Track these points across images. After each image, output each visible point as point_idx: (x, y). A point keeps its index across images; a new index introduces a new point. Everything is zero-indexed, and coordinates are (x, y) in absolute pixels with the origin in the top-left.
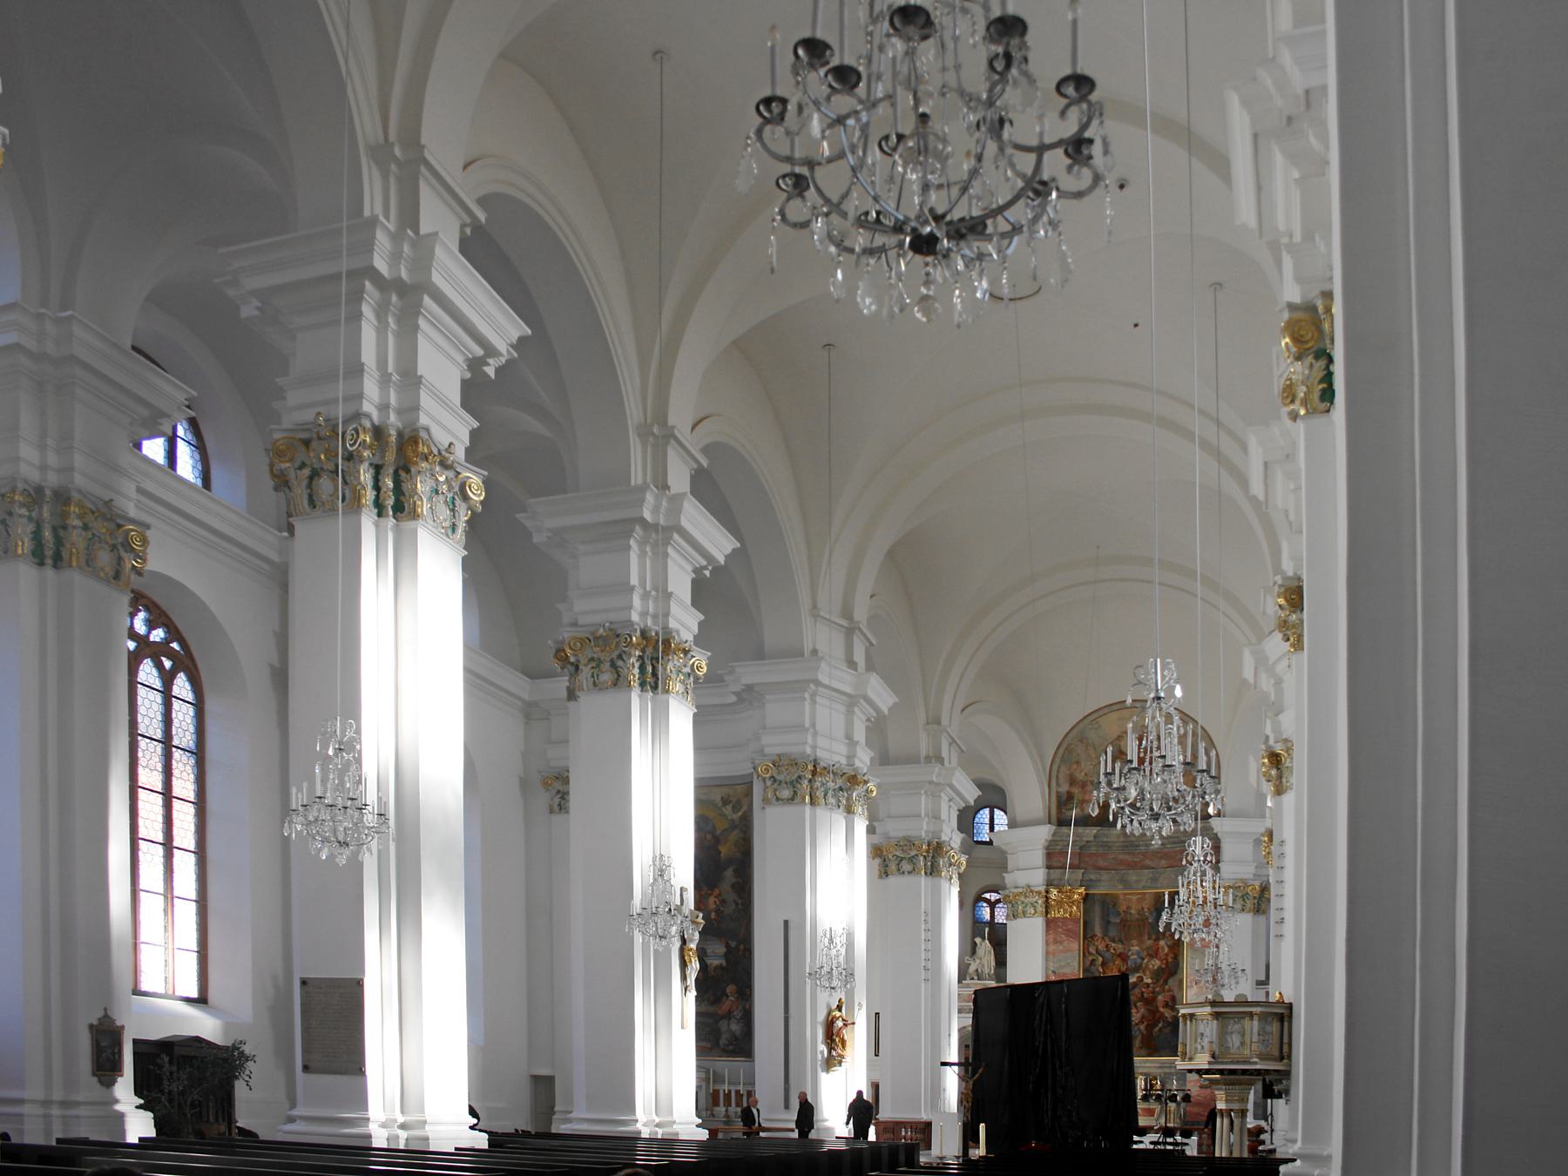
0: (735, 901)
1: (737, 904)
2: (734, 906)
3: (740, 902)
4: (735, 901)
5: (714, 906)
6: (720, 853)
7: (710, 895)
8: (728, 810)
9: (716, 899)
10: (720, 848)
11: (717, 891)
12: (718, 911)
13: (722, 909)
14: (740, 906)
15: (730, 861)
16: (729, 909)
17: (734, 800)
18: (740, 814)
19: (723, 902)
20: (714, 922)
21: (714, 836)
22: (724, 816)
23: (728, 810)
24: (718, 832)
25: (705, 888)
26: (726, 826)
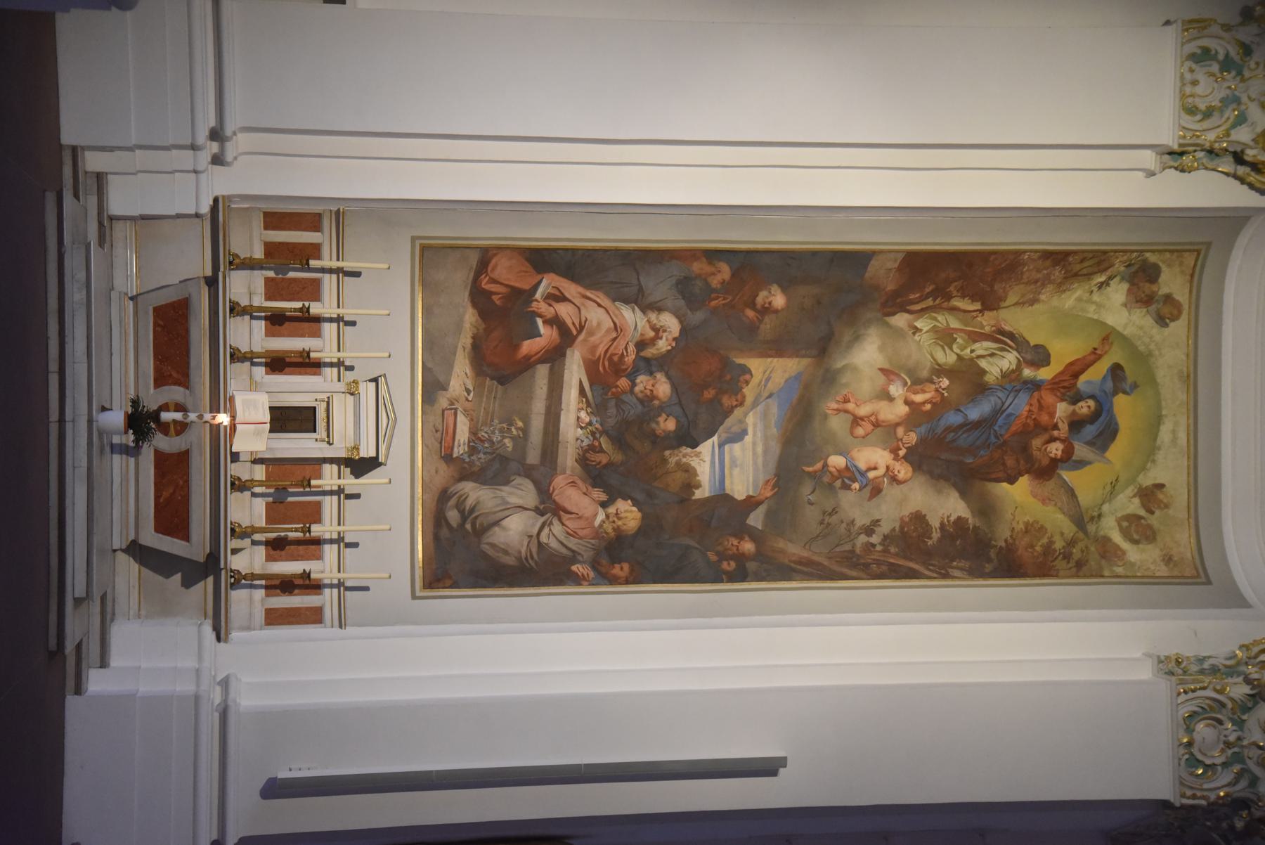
0: (876, 522)
1: (869, 531)
2: (862, 520)
3: (875, 539)
4: (876, 522)
5: (862, 466)
6: (1012, 481)
7: (894, 451)
8: (1128, 503)
9: (881, 471)
10: (1024, 481)
11: (903, 471)
12: (850, 474)
13: (856, 486)
14: (863, 539)
15: (986, 509)
16: (854, 507)
17: (1154, 520)
18: (1117, 538)
19: (876, 491)
20: (819, 466)
21: (1055, 463)
22: (1113, 489)
23: (1128, 503)
24: (1067, 475)
25: (912, 438)
26: (1086, 497)
